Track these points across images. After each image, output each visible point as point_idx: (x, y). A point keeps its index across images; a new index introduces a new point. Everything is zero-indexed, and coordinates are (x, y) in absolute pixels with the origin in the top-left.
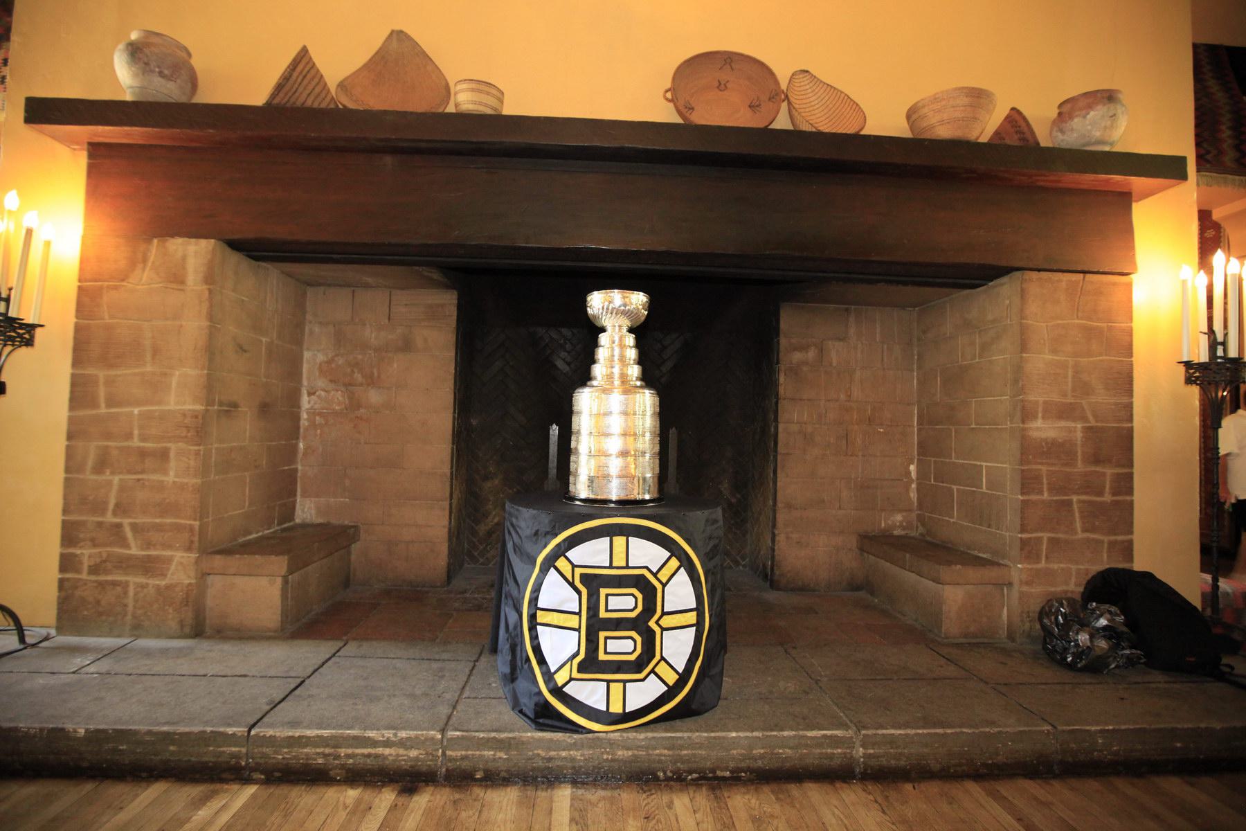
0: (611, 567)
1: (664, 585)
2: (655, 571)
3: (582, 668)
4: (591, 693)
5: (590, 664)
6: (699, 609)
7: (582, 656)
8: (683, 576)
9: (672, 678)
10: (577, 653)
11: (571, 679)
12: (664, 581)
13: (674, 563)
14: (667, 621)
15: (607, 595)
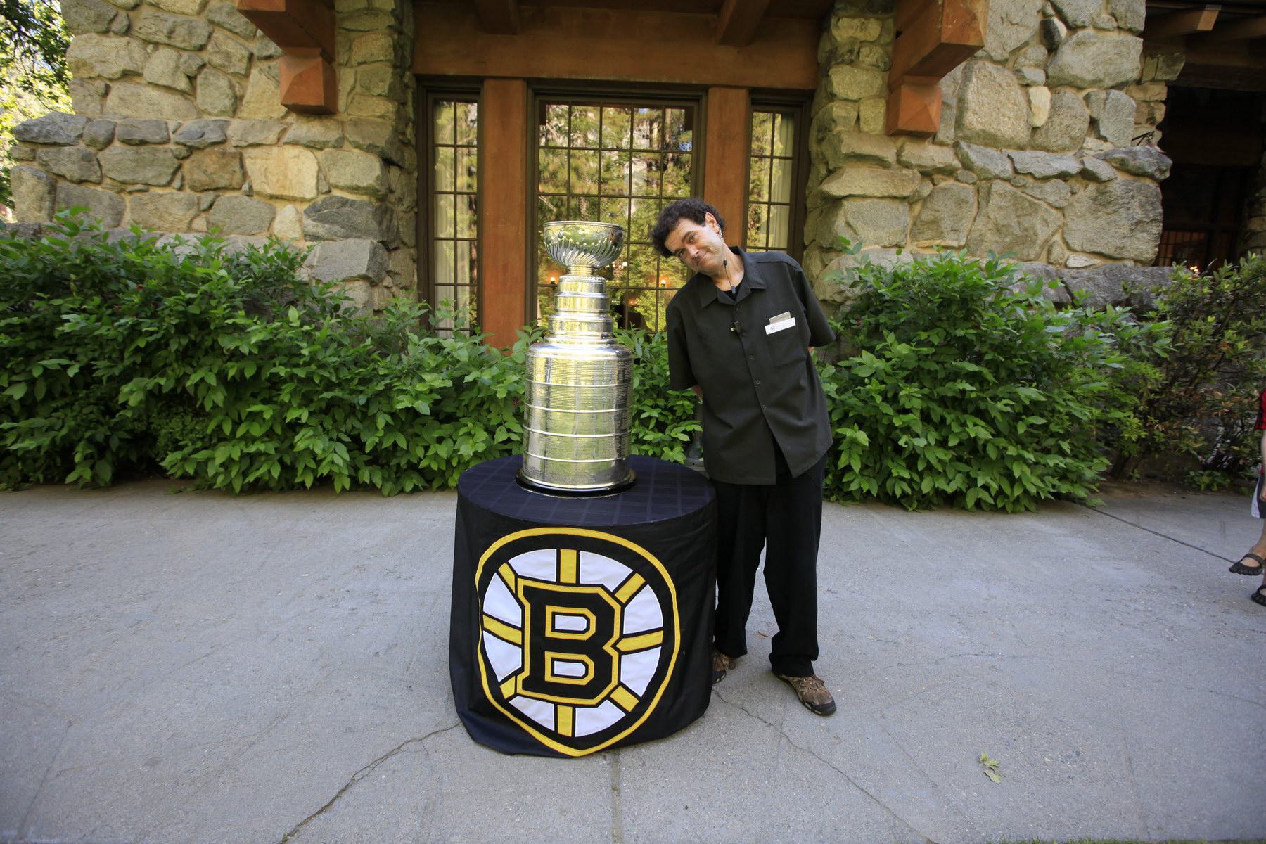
0: (558, 583)
1: (623, 606)
2: (612, 590)
3: (527, 685)
4: (539, 710)
5: (536, 683)
6: (668, 628)
7: (526, 673)
8: (649, 594)
9: (630, 703)
10: (521, 670)
11: (516, 695)
12: (624, 601)
13: (638, 580)
14: (625, 645)
15: (554, 614)
